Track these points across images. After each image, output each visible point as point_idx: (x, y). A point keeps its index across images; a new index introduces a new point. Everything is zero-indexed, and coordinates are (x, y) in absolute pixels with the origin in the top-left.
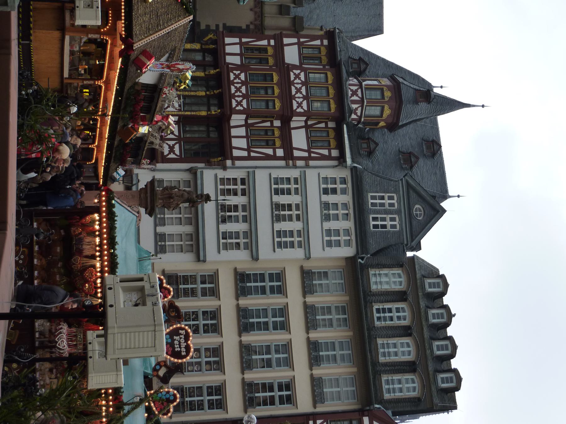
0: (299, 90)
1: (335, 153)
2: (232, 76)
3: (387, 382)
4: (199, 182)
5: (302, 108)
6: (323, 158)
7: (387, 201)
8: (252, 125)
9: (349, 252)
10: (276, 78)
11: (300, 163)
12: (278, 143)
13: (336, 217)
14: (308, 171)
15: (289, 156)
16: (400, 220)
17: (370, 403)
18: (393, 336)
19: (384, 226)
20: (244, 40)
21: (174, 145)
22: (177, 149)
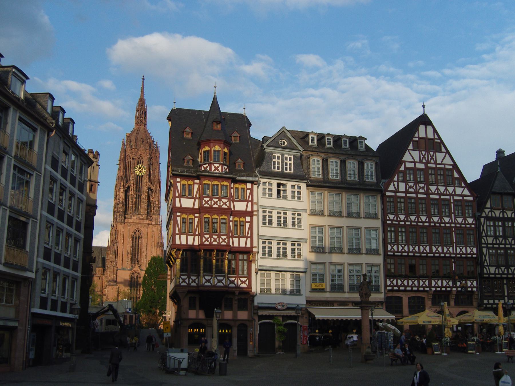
0: (216, 203)
1: (249, 185)
2: (207, 243)
3: (368, 178)
4: (265, 268)
5: (226, 202)
6: (252, 193)
9: (304, 186)
11: (255, 208)
12: (242, 219)
15: (251, 214)
16: (288, 154)
19: (290, 164)
20: (177, 232)
21: (241, 281)
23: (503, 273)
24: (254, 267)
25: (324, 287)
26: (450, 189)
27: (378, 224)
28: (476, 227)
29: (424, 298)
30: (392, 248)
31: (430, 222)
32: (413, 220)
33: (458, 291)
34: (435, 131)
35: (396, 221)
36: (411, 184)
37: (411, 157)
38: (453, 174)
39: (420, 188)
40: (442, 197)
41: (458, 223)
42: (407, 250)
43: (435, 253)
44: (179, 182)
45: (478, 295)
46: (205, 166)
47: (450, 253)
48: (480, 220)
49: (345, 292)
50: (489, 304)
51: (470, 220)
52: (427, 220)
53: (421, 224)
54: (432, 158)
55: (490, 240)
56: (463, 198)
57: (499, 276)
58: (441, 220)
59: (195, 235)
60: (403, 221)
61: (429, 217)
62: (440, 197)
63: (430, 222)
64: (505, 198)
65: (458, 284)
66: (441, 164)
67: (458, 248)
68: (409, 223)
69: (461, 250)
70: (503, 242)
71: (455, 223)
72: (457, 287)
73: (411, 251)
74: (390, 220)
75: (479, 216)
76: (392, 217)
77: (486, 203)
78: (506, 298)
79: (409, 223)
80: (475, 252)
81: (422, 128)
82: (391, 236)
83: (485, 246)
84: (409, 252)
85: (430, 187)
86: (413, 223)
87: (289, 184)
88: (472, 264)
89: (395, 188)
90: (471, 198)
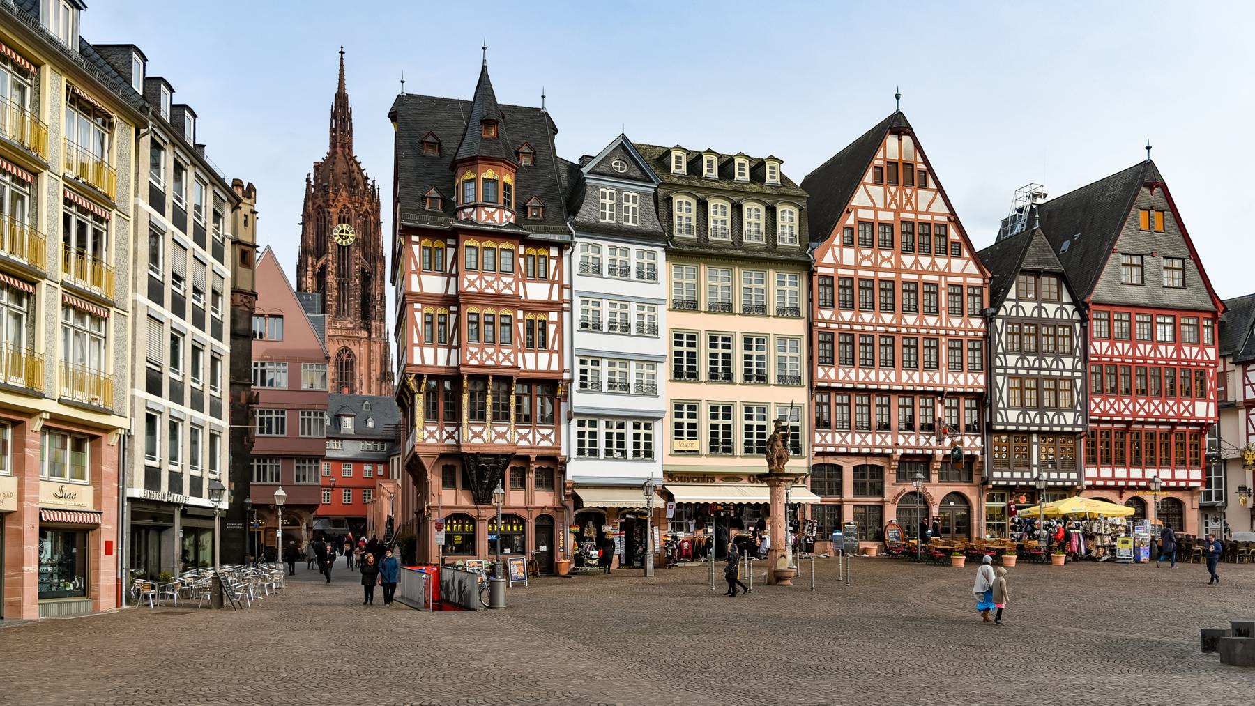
0: (489, 284)
1: (554, 252)
8: (522, 344)
9: (661, 254)
10: (472, 309)
11: (566, 296)
12: (541, 317)
15: (558, 307)
19: (634, 210)
20: (416, 341)
22: (546, 432)
23: (1032, 424)
24: (564, 407)
25: (696, 448)
26: (941, 262)
27: (797, 327)
29: (882, 468)
30: (826, 374)
33: (946, 456)
34: (918, 146)
35: (836, 322)
36: (866, 252)
37: (869, 200)
38: (946, 236)
39: (884, 259)
41: (952, 329)
44: (415, 243)
45: (982, 462)
46: (468, 211)
50: (1002, 479)
51: (977, 323)
53: (882, 329)
54: (909, 201)
55: (1012, 360)
57: (1025, 428)
59: (450, 347)
60: (849, 323)
64: (1045, 280)
65: (947, 442)
66: (927, 213)
68: (859, 328)
69: (956, 379)
70: (1036, 365)
72: (944, 449)
73: (861, 379)
76: (827, 314)
77: (1007, 290)
78: (1035, 470)
79: (859, 328)
81: (891, 141)
83: (1002, 371)
85: (904, 258)
86: (867, 328)
88: (974, 405)
89: (835, 258)
90: (979, 281)
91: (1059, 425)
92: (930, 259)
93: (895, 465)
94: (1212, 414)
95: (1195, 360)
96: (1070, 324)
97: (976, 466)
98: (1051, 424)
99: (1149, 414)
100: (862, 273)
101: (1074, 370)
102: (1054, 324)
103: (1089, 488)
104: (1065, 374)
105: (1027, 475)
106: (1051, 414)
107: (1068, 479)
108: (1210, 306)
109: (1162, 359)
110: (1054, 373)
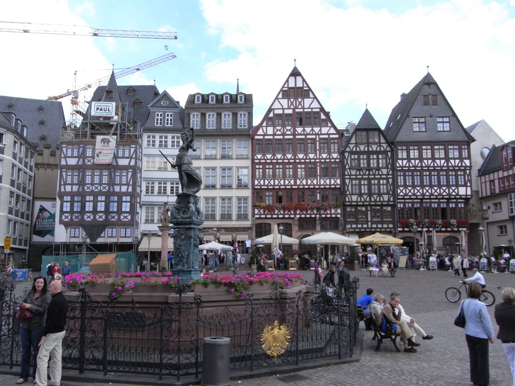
4: (147, 203)
7: (159, 117)
13: (166, 142)
14: (143, 153)
17: (249, 135)
18: (221, 121)
19: (171, 120)
23: (365, 201)
26: (317, 130)
27: (248, 163)
28: (340, 161)
31: (295, 159)
32: (279, 158)
34: (304, 80)
35: (264, 159)
39: (287, 130)
40: (308, 137)
41: (323, 159)
42: (272, 184)
43: (300, 185)
47: (314, 185)
48: (344, 154)
49: (216, 220)
51: (335, 156)
52: (293, 158)
53: (287, 161)
54: (300, 103)
55: (353, 172)
56: (329, 136)
58: (306, 157)
60: (270, 159)
61: (295, 155)
62: (306, 137)
63: (295, 159)
66: (309, 108)
67: (322, 180)
69: (325, 182)
70: (367, 173)
71: (320, 159)
73: (276, 184)
74: (258, 159)
75: (343, 151)
76: (259, 156)
78: (370, 223)
79: (275, 161)
80: (339, 183)
82: (259, 173)
83: (348, 177)
84: (274, 185)
85: (297, 129)
86: (279, 161)
87: (170, 136)
89: (264, 132)
90: (337, 136)
91: (380, 201)
92: (311, 128)
93: (297, 223)
94: (469, 193)
95: (457, 166)
96: (385, 152)
97: (340, 222)
98: (375, 201)
99: (432, 194)
100: (276, 137)
101: (388, 174)
102: (377, 153)
103: (400, 231)
104: (383, 176)
105: (365, 226)
106: (375, 196)
107: (388, 228)
108: (465, 138)
109: (438, 166)
110: (376, 177)
